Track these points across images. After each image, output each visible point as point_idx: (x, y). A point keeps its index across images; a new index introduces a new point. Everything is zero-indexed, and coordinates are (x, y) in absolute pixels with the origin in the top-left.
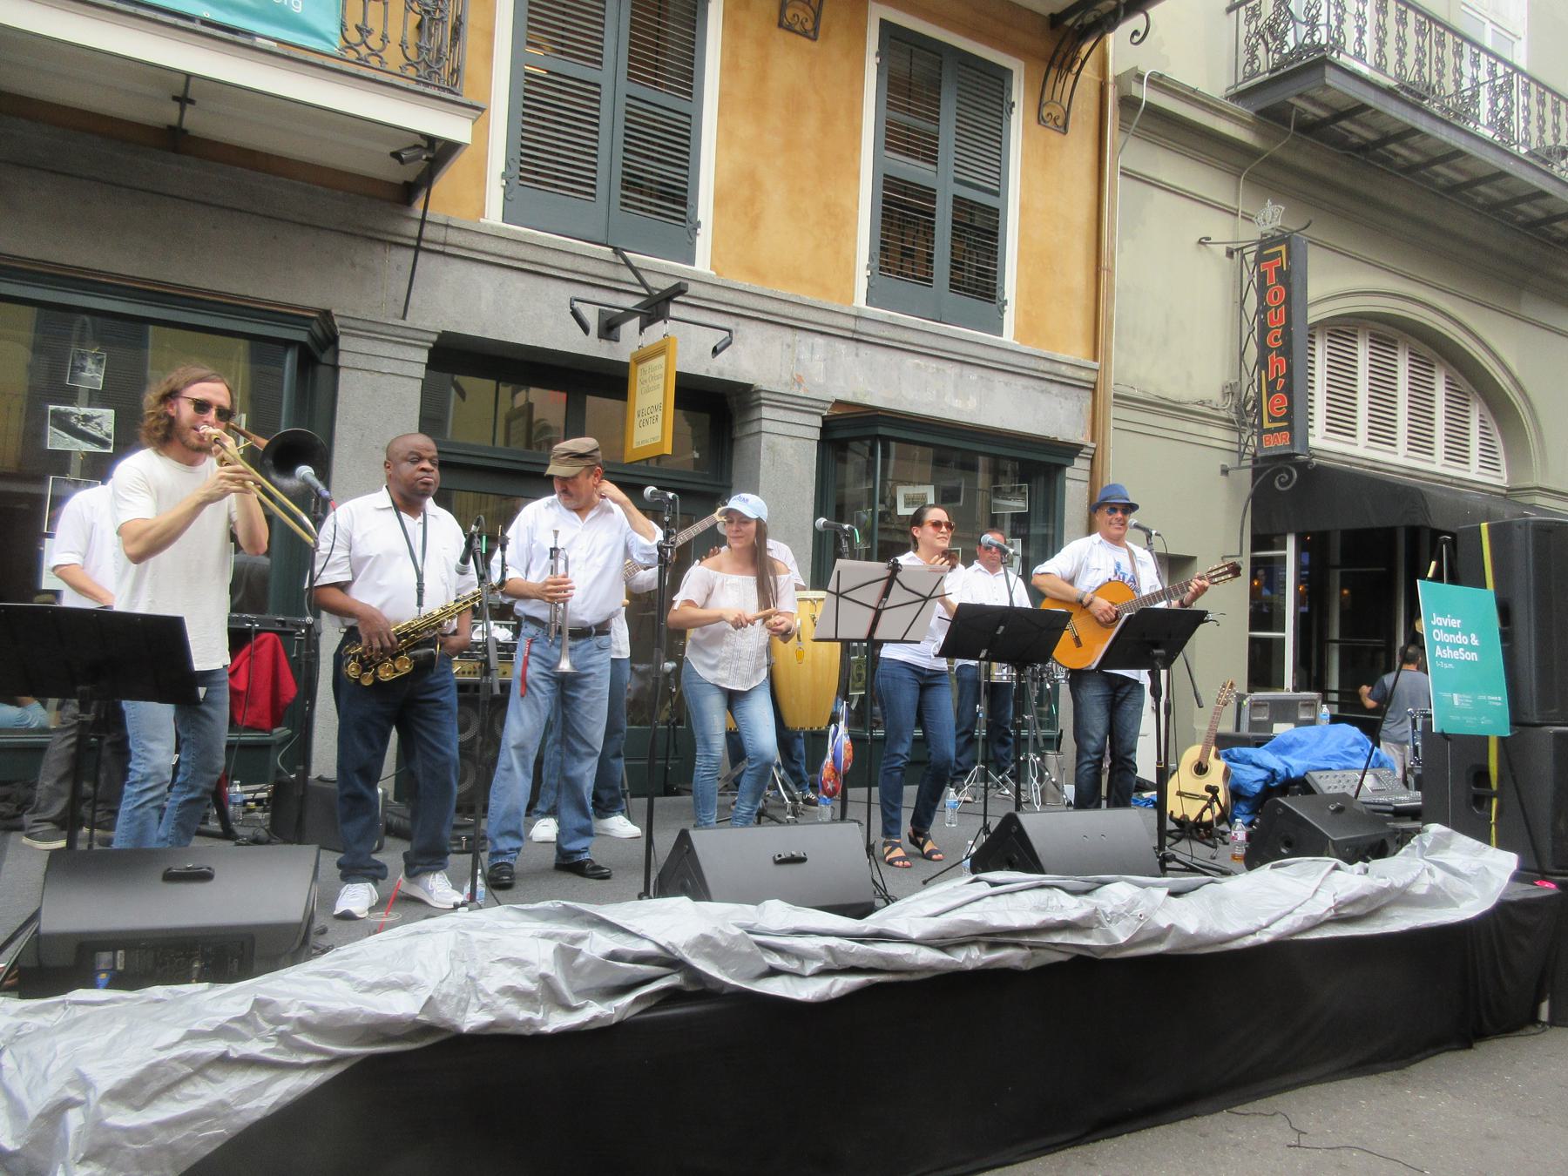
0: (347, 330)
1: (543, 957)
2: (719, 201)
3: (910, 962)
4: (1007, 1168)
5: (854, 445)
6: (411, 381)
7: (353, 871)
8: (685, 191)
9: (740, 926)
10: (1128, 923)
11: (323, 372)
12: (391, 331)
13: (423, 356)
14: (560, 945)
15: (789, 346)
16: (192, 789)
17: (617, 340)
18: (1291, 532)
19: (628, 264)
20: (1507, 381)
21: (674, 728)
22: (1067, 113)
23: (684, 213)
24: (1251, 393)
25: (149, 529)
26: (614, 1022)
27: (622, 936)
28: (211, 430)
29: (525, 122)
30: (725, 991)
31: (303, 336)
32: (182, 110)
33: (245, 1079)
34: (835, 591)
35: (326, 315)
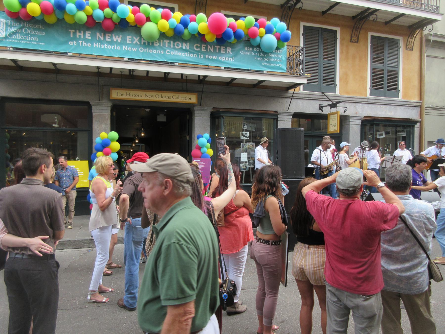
5: (367, 125)
12: (286, 113)
13: (291, 117)
15: (354, 106)
19: (325, 95)
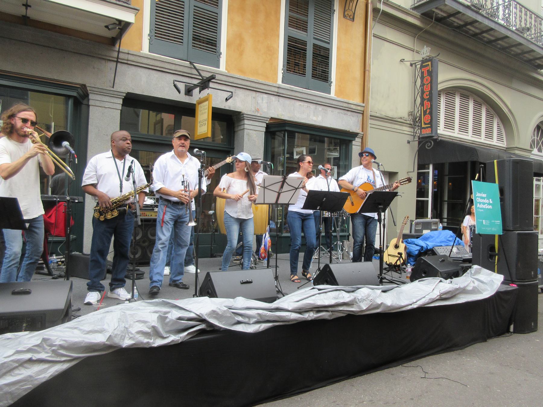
0: (92, 92)
1: (153, 319)
2: (228, 45)
3: (288, 318)
4: (323, 388)
5: (278, 133)
6: (117, 111)
7: (92, 287)
8: (216, 41)
9: (226, 307)
10: (366, 303)
11: (84, 107)
14: (160, 315)
15: (254, 98)
16: (31, 259)
17: (192, 96)
18: (431, 163)
20: (507, 110)
21: (214, 234)
22: (354, 14)
23: (216, 49)
24: (418, 115)
25: (9, 167)
26: (180, 342)
27: (183, 311)
28: (28, 130)
29: (156, 15)
30: (221, 330)
31: (75, 94)
32: (26, 9)
33: (39, 367)
34: (263, 186)
35: (84, 86)
